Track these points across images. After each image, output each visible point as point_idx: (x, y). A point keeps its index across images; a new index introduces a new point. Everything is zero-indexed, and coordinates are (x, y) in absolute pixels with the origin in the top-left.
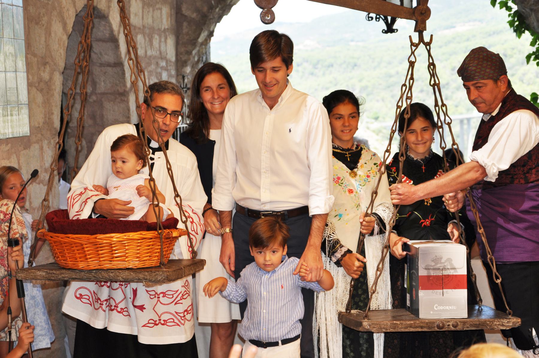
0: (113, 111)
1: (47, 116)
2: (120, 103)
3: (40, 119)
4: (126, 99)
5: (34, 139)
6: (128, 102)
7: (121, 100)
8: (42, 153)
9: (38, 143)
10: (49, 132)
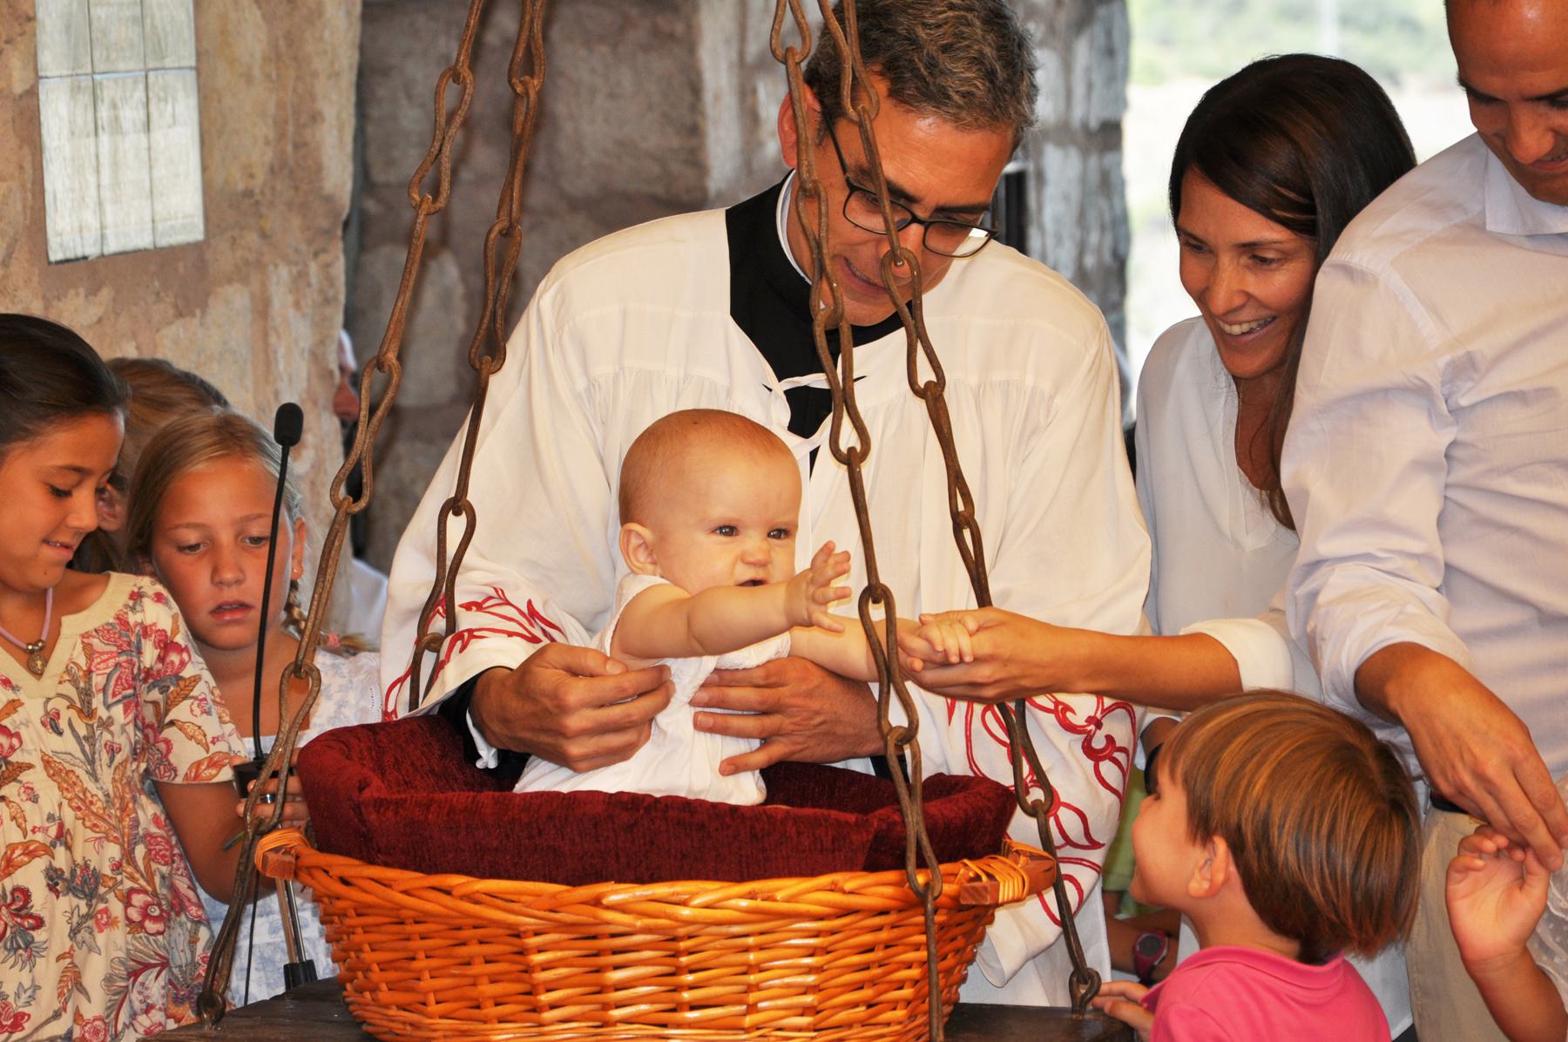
0: (612, 96)
1: (291, 129)
2: (646, 49)
3: (255, 148)
4: (679, 28)
5: (224, 258)
6: (690, 43)
7: (656, 32)
8: (266, 335)
9: (245, 281)
10: (296, 222)
